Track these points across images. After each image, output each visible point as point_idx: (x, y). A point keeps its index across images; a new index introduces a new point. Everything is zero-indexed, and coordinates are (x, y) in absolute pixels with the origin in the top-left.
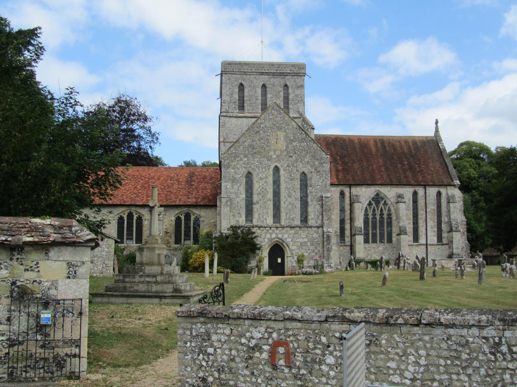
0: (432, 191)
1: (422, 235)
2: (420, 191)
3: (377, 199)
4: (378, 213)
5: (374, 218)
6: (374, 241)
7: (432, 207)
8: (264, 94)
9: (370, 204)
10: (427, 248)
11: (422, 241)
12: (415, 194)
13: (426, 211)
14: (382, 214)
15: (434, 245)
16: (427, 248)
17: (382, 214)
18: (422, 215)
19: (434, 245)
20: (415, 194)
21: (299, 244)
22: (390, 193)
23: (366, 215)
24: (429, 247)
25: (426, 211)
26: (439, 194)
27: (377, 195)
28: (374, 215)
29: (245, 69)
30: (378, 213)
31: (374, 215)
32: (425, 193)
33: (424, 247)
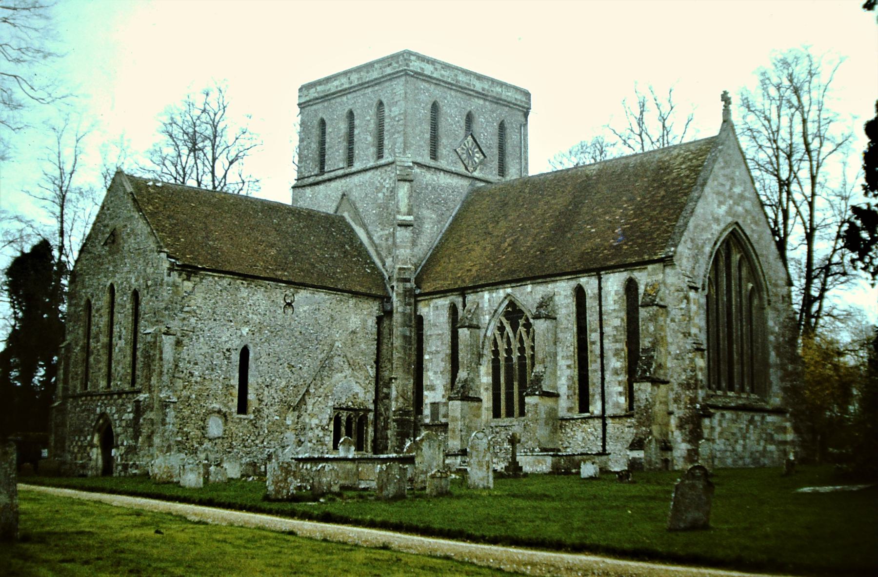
0: (614, 283)
1: (593, 396)
2: (589, 284)
3: (514, 313)
4: (515, 345)
5: (509, 359)
6: (510, 414)
7: (615, 322)
8: (352, 128)
9: (501, 329)
10: (604, 425)
11: (596, 408)
12: (580, 293)
13: (602, 334)
14: (522, 350)
15: (620, 417)
16: (604, 425)
17: (522, 350)
18: (593, 343)
19: (620, 417)
20: (580, 293)
21: (124, 424)
22: (529, 295)
23: (496, 353)
24: (609, 421)
25: (602, 334)
26: (631, 287)
27: (512, 304)
28: (509, 351)
29: (333, 86)
30: (515, 345)
31: (509, 351)
32: (600, 288)
33: (598, 423)
